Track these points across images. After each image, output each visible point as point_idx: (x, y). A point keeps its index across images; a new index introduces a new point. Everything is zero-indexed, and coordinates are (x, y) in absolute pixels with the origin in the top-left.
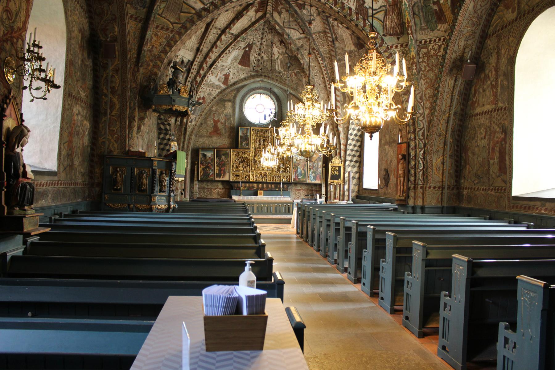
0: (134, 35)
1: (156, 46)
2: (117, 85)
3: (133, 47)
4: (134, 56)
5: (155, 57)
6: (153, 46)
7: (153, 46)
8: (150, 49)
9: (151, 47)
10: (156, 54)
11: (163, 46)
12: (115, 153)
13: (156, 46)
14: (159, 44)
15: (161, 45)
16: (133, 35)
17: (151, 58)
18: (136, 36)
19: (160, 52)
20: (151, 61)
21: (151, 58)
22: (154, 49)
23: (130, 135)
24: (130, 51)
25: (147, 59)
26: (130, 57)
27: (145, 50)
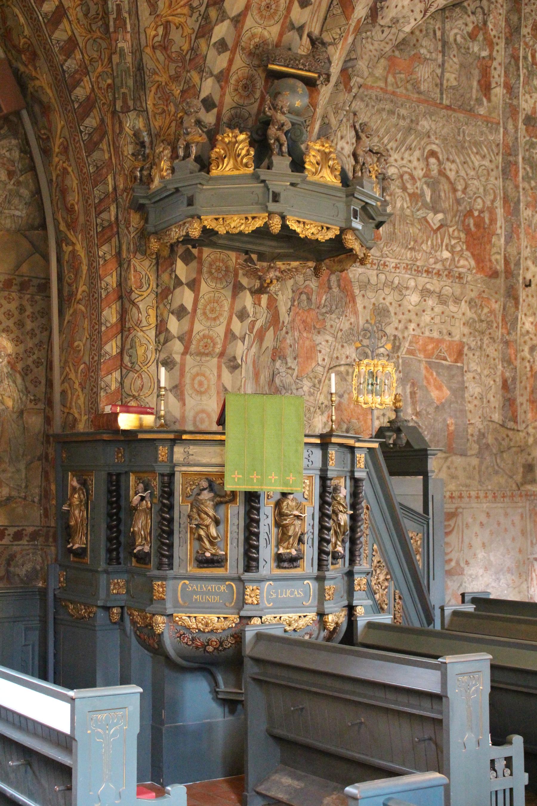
0: (86, 15)
1: (177, 20)
2: (76, 200)
3: (95, 55)
4: (103, 85)
5: (183, 60)
6: (167, 25)
7: (167, 25)
8: (158, 39)
9: (161, 30)
10: (186, 47)
11: (203, 9)
12: (81, 427)
13: (177, 20)
14: (186, 10)
15: (192, 8)
16: (80, 15)
17: (172, 72)
18: (93, 12)
19: (196, 38)
20: (175, 78)
21: (172, 72)
22: (175, 35)
23: (126, 359)
24: (88, 73)
25: (163, 79)
26: (93, 90)
27: (122, 50)
